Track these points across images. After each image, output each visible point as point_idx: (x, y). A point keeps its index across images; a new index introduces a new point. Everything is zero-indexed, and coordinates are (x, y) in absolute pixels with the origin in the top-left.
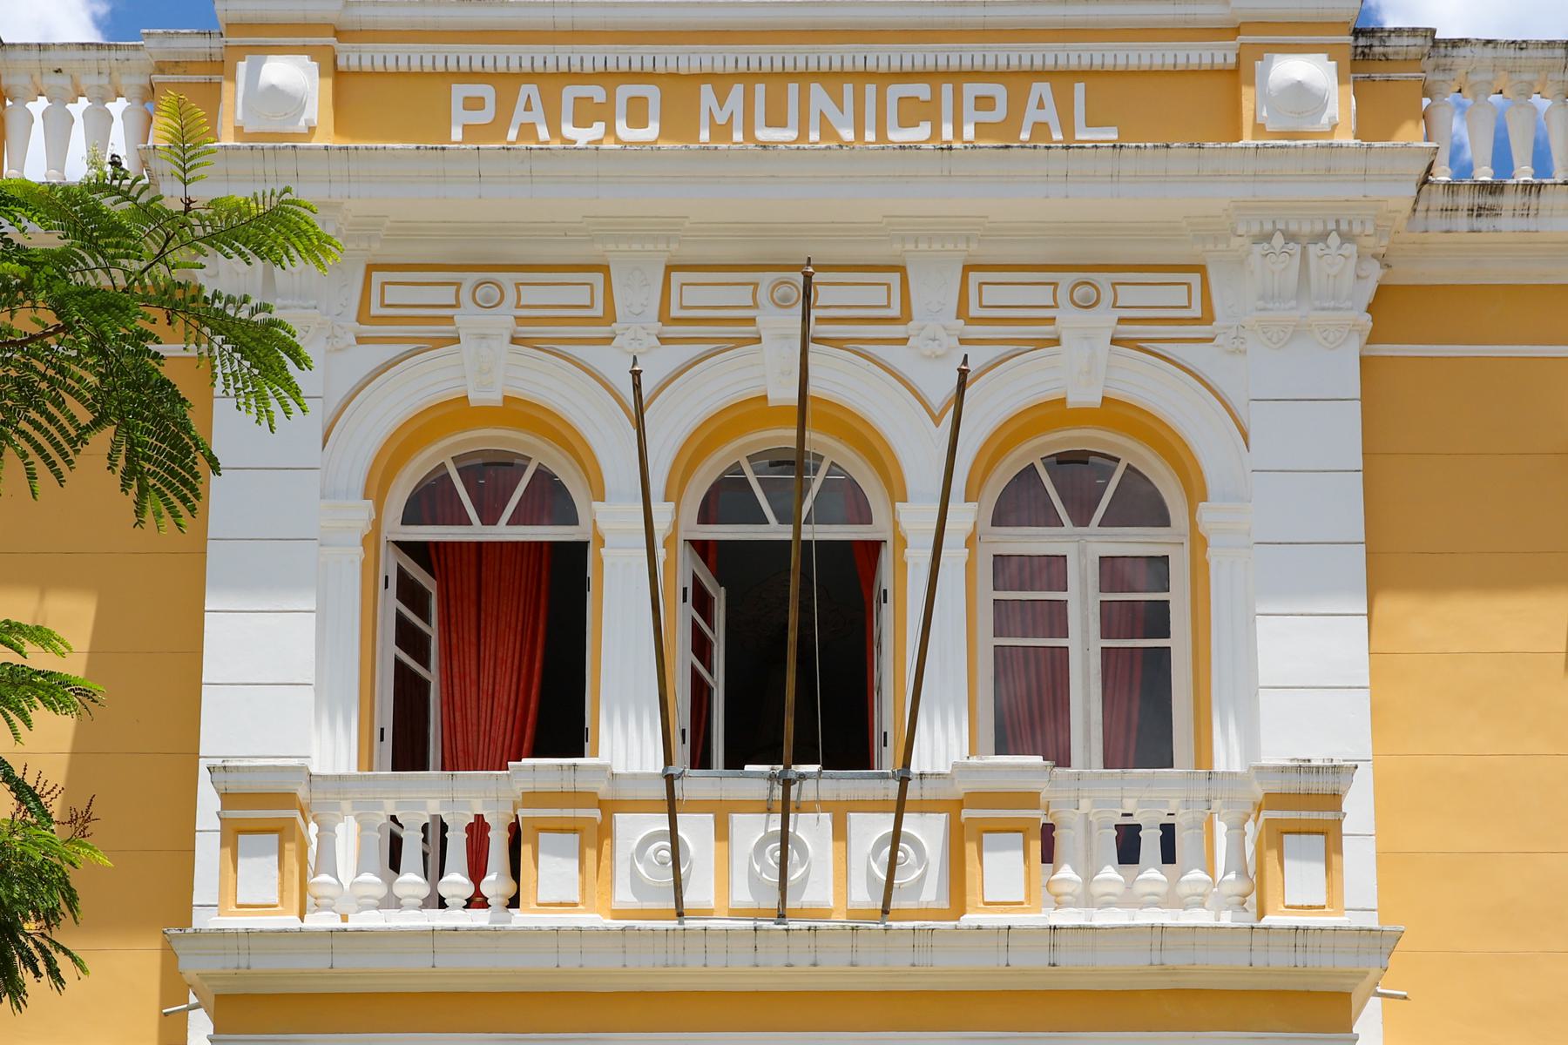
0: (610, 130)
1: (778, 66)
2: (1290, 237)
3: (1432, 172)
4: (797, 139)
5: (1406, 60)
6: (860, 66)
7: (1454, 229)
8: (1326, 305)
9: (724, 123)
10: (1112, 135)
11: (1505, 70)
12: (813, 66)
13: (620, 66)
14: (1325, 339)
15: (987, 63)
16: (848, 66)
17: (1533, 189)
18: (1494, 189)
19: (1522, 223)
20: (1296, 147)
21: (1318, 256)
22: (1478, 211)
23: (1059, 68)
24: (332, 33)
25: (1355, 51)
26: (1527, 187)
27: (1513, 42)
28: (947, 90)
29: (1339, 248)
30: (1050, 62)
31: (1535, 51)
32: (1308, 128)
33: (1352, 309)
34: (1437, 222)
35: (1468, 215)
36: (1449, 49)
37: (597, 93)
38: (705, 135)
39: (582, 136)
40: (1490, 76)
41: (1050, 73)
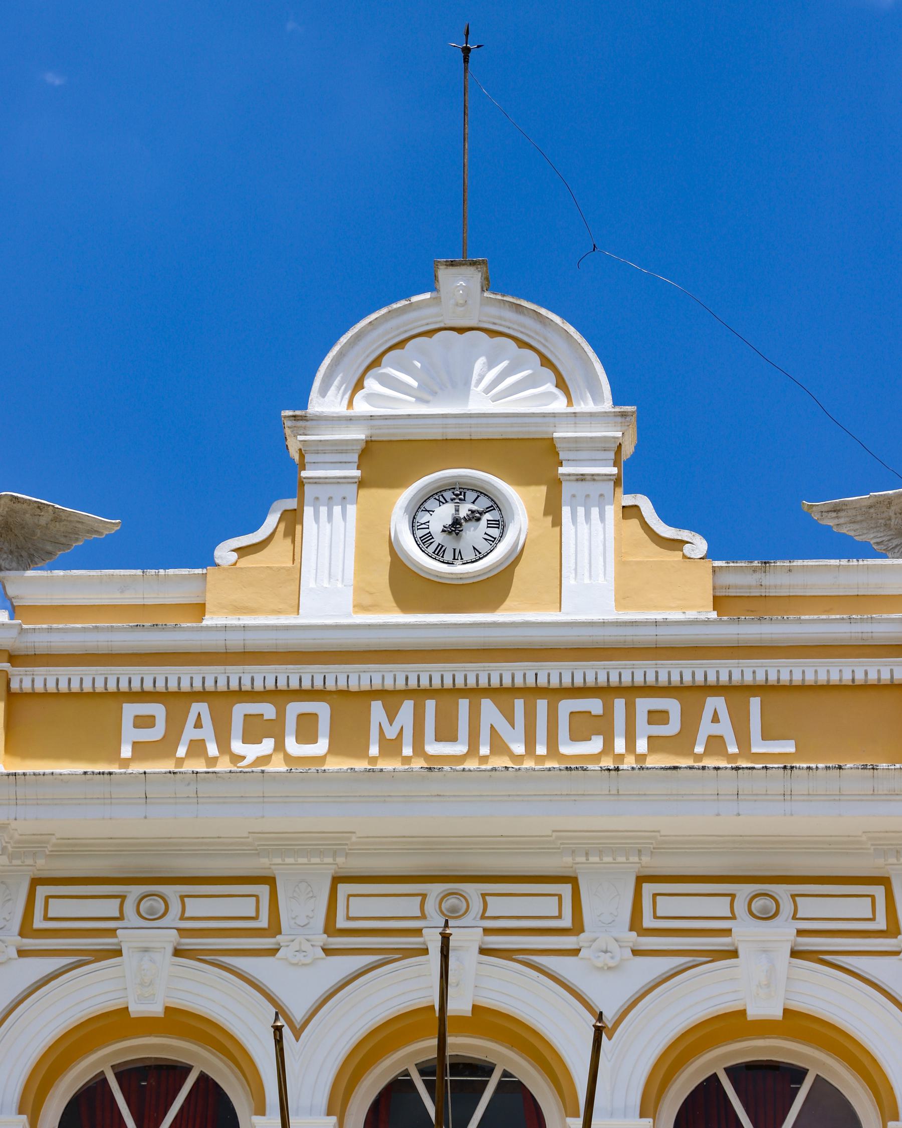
0: (280, 746)
1: (448, 683)
4: (467, 753)
6: (531, 682)
9: (394, 738)
10: (789, 747)
12: (483, 683)
13: (290, 685)
15: (660, 679)
16: (519, 682)
23: (734, 683)
24: (6, 657)
28: (619, 704)
30: (724, 679)
37: (268, 710)
38: (374, 750)
39: (251, 752)
41: (724, 687)
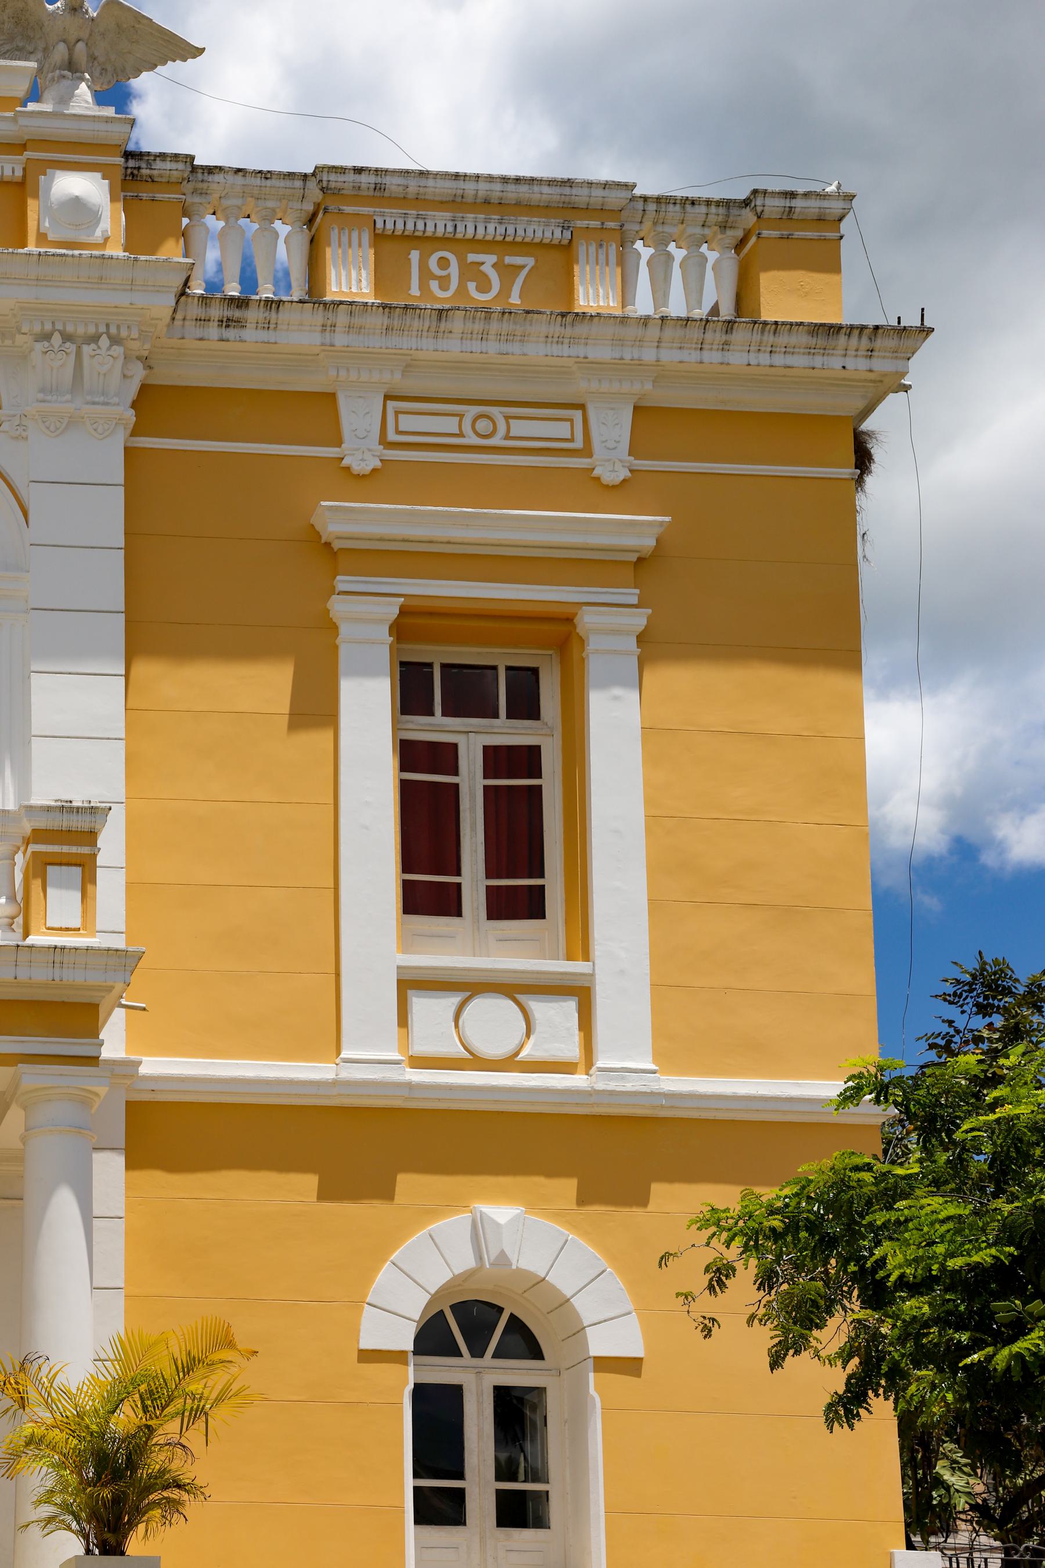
2: (67, 338)
3: (189, 284)
5: (168, 182)
7: (206, 337)
8: (97, 400)
11: (252, 197)
14: (95, 430)
17: (274, 305)
18: (241, 303)
19: (263, 335)
20: (73, 256)
21: (90, 356)
22: (227, 323)
25: (126, 171)
26: (268, 302)
27: (260, 172)
29: (109, 349)
31: (278, 180)
32: (83, 238)
33: (118, 404)
34: (192, 330)
35: (218, 325)
36: (206, 174)
40: (238, 202)
